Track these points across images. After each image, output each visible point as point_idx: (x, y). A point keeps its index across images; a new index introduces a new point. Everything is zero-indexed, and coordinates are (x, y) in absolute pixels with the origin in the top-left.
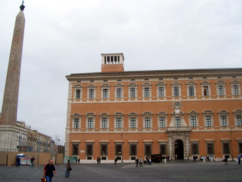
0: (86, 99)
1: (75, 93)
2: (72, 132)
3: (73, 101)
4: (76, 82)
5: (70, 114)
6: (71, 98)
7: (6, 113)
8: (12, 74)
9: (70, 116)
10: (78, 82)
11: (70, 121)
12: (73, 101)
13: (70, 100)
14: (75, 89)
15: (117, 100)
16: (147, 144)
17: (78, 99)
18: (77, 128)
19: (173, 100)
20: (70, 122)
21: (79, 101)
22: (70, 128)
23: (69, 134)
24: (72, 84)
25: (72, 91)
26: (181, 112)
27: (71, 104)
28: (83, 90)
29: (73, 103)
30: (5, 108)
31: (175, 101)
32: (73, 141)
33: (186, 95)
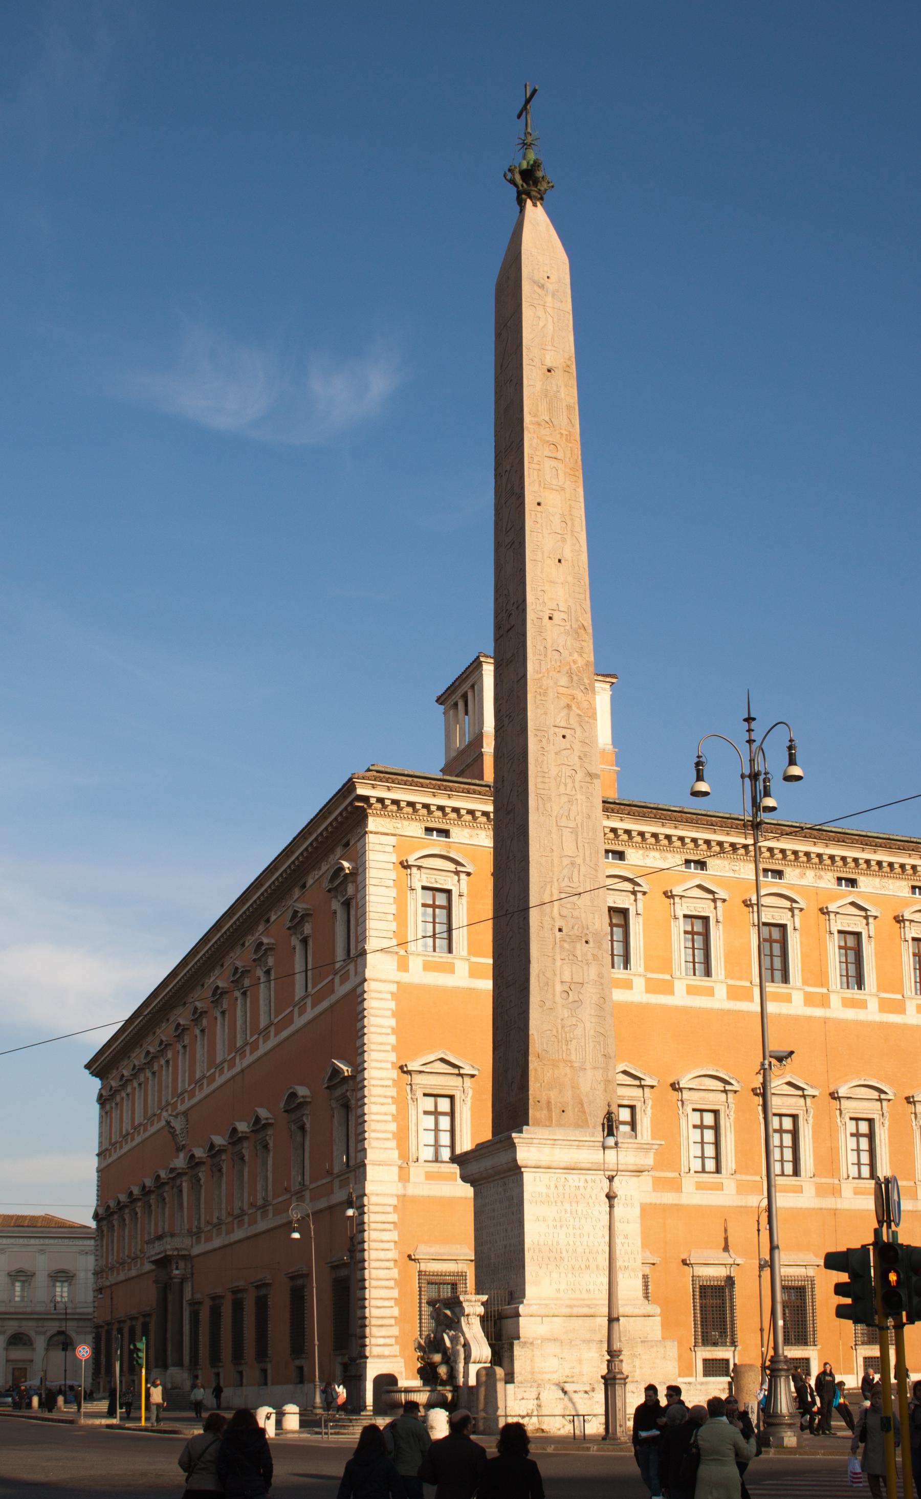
2: (412, 1190)
3: (403, 966)
4: (415, 829)
5: (393, 1057)
7: (578, 1031)
9: (395, 1074)
10: (429, 830)
11: (393, 1109)
12: (403, 966)
20: (395, 1118)
21: (450, 969)
24: (392, 840)
25: (393, 893)
29: (405, 978)
30: (559, 988)
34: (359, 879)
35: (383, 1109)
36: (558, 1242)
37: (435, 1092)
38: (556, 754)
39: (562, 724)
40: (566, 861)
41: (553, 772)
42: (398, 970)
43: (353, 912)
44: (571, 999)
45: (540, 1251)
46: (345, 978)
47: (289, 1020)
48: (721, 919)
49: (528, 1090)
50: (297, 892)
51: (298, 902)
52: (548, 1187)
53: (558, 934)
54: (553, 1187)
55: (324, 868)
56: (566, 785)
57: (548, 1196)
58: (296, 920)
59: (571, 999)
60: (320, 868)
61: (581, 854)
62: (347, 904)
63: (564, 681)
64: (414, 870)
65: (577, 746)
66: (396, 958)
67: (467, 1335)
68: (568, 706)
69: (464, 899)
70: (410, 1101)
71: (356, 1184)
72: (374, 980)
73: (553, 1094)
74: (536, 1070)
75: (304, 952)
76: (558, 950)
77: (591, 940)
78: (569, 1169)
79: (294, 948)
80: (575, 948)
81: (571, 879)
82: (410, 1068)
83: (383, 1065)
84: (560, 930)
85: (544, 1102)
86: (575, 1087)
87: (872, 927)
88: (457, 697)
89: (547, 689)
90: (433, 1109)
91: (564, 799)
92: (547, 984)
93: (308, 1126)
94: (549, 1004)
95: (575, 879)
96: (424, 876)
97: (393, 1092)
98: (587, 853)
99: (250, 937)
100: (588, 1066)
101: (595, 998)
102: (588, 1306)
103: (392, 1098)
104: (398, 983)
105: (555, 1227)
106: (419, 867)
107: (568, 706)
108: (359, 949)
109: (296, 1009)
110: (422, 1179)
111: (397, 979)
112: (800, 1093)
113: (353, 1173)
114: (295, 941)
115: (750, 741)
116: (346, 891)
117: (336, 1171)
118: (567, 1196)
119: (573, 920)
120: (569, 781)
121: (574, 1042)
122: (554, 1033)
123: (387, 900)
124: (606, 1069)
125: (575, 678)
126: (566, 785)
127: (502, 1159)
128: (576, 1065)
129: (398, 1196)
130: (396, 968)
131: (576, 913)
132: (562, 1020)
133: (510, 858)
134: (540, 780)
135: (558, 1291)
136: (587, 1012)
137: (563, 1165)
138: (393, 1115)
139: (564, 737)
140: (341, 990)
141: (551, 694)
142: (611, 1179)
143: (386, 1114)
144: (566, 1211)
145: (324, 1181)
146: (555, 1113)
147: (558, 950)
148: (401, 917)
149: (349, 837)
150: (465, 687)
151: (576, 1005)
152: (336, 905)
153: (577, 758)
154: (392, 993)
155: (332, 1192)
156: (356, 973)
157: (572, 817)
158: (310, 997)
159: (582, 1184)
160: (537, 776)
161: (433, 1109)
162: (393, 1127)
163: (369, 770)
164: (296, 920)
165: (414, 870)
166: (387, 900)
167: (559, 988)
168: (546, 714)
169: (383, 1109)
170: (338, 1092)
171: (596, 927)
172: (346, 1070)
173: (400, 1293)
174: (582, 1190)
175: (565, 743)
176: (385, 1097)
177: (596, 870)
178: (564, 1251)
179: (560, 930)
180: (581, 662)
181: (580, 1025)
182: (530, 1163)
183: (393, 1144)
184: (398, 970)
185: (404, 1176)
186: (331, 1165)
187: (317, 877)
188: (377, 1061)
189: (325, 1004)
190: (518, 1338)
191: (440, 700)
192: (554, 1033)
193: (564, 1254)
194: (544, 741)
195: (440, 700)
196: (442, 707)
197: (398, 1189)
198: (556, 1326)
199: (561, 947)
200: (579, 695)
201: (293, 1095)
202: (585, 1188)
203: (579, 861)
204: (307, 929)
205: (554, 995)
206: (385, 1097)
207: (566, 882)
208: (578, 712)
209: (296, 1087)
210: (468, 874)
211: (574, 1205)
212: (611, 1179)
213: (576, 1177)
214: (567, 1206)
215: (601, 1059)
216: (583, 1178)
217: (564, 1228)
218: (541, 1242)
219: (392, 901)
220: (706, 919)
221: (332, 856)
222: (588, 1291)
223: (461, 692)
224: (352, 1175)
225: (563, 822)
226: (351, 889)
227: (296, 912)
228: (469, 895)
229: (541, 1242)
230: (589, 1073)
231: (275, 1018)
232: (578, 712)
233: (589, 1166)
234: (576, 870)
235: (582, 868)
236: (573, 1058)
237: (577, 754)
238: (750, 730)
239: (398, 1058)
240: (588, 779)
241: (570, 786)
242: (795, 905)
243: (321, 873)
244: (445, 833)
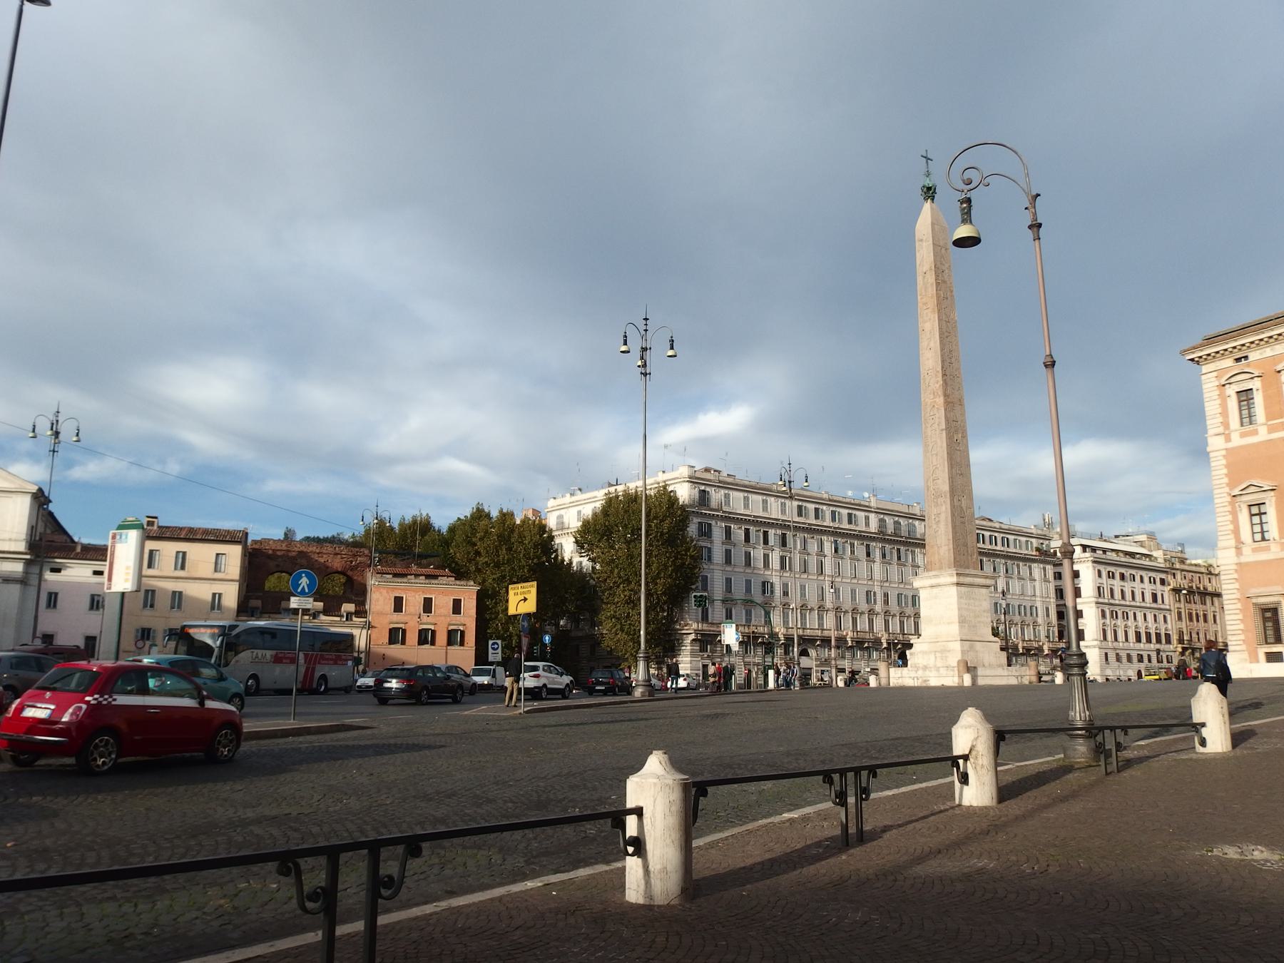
1: (1233, 403)
2: (1243, 559)
3: (1228, 439)
4: (1228, 362)
5: (1227, 489)
6: (1221, 430)
7: (940, 532)
8: (935, 412)
9: (1229, 499)
10: (1238, 360)
11: (1230, 517)
12: (1228, 439)
14: (1231, 391)
17: (1248, 428)
18: (1263, 539)
21: (1255, 433)
23: (1235, 567)
24: (1215, 374)
25: (1218, 402)
28: (1265, 388)
29: (1230, 445)
32: (1253, 591)
41: (929, 434)
72: (1213, 451)
83: (1222, 495)
86: (939, 554)
100: (943, 544)
103: (1229, 511)
104: (1226, 449)
107: (934, 406)
111: (1225, 447)
129: (1237, 564)
130: (1224, 441)
148: (1225, 413)
162: (1231, 527)
180: (938, 386)
197: (1235, 560)
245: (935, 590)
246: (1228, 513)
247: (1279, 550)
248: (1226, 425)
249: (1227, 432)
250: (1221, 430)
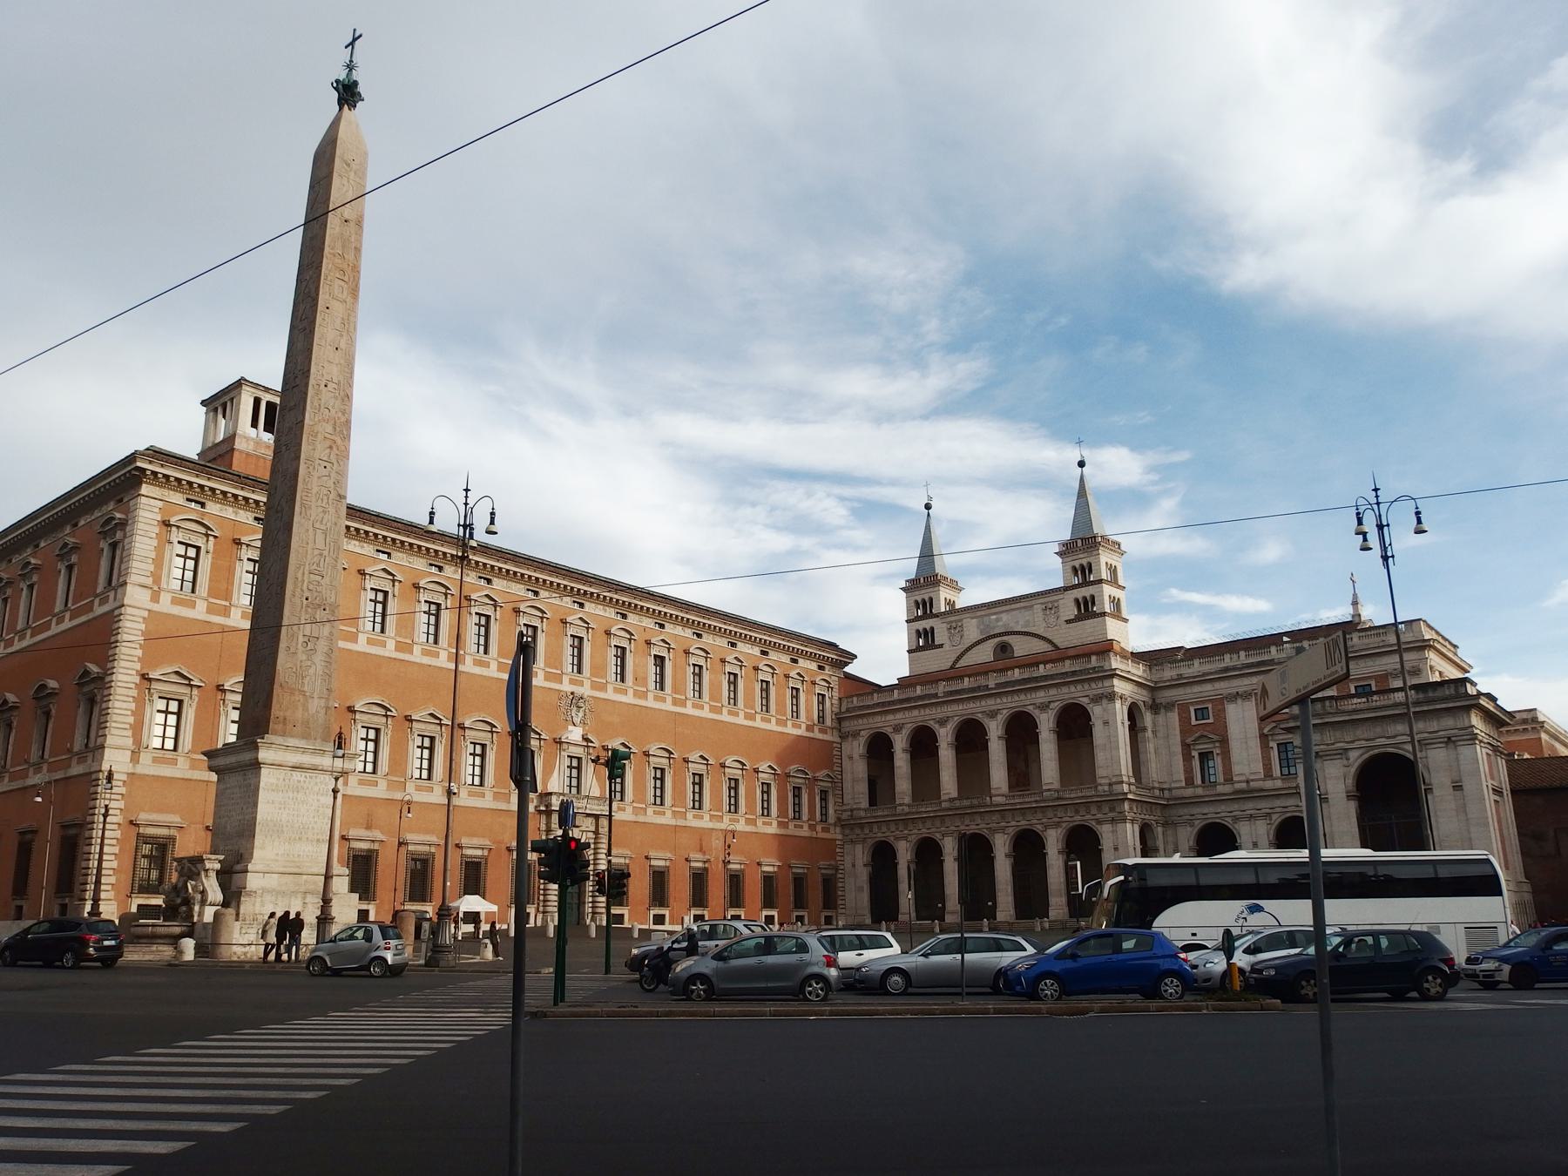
0: (224, 603)
2: (139, 770)
3: (155, 598)
4: (178, 498)
5: (138, 666)
6: (149, 581)
7: (311, 671)
9: (137, 679)
12: (155, 598)
13: (145, 590)
15: (370, 642)
16: (471, 857)
19: (566, 687)
20: (134, 713)
22: (129, 742)
24: (160, 504)
26: (586, 739)
27: (146, 614)
29: (155, 607)
30: (301, 639)
31: (572, 693)
32: (143, 817)
33: (605, 676)
34: (128, 528)
35: (125, 705)
36: (281, 820)
37: (169, 696)
38: (319, 478)
39: (324, 459)
40: (316, 552)
42: (151, 601)
43: (118, 552)
44: (309, 648)
45: (267, 825)
46: (104, 601)
47: (47, 626)
48: (396, 594)
49: (270, 709)
50: (68, 530)
51: (68, 536)
52: (278, 779)
53: (305, 602)
54: (281, 780)
55: (97, 514)
56: (322, 500)
57: (277, 785)
58: (65, 550)
59: (309, 648)
60: (92, 514)
61: (327, 548)
62: (114, 546)
63: (329, 429)
64: (174, 529)
65: (333, 475)
66: (150, 591)
67: (206, 885)
68: (331, 447)
69: (210, 556)
70: (147, 701)
71: (93, 761)
72: (130, 606)
73: (288, 714)
74: (278, 695)
75: (67, 577)
76: (303, 613)
77: (327, 609)
78: (295, 767)
79: (60, 572)
80: (316, 613)
81: (318, 565)
82: (151, 676)
83: (130, 672)
84: (307, 599)
85: (281, 719)
86: (306, 709)
87: (498, 613)
88: (217, 404)
89: (317, 433)
90: (164, 709)
91: (321, 509)
92: (293, 635)
93: (53, 711)
94: (292, 650)
95: (321, 566)
96: (180, 534)
97: (134, 693)
98: (332, 550)
99: (17, 556)
100: (315, 695)
101: (326, 649)
102: (298, 867)
103: (133, 697)
104: (149, 610)
105: (280, 809)
106: (178, 527)
107: (331, 447)
108: (121, 580)
109: (54, 620)
110: (149, 762)
111: (148, 608)
112: (438, 722)
113: (92, 753)
114: (62, 567)
115: (466, 504)
116: (115, 535)
117: (75, 749)
118: (291, 787)
119: (317, 594)
120: (325, 498)
121: (308, 678)
122: (294, 670)
123: (149, 548)
124: (327, 699)
125: (338, 429)
126: (322, 500)
127: (246, 757)
128: (307, 694)
129: (128, 774)
131: (319, 589)
132: (301, 661)
133: (276, 543)
134: (306, 494)
135: (277, 854)
136: (319, 659)
137: (290, 764)
138: (132, 711)
139: (325, 467)
140: (99, 610)
141: (320, 437)
142: (337, 779)
143: (126, 709)
144: (289, 798)
145: (64, 757)
146: (289, 726)
147: (303, 613)
148: (159, 562)
149: (122, 495)
150: (226, 398)
151: (312, 652)
152: (104, 545)
153: (332, 483)
154: (144, 618)
155: (69, 766)
156: (115, 599)
157: (324, 523)
158: (69, 612)
159: (302, 779)
160: (302, 491)
161: (164, 709)
162: (131, 720)
163: (147, 449)
164: (65, 550)
165: (174, 529)
166: (149, 548)
167: (301, 639)
168: (314, 449)
169: (125, 705)
170: (86, 689)
171: (332, 600)
172: (94, 668)
173: (120, 850)
174: (302, 783)
175: (325, 472)
176: (128, 696)
177: (336, 561)
178: (284, 825)
179: (307, 599)
181: (314, 667)
182: (267, 761)
183: (129, 733)
184: (151, 601)
185: (135, 756)
186: (72, 745)
187: (89, 520)
188: (125, 668)
189: (83, 619)
190: (245, 888)
191: (204, 403)
192: (294, 670)
193: (285, 829)
194: (311, 468)
195: (204, 403)
196: (205, 408)
197: (129, 768)
198: (272, 881)
199: (306, 612)
200: (339, 441)
201: (44, 686)
202: (305, 782)
203: (325, 553)
204: (74, 558)
205: (297, 644)
206: (128, 696)
207: (315, 567)
208: (337, 452)
209: (49, 681)
210: (215, 537)
211: (295, 793)
212: (337, 779)
213: (298, 773)
214: (291, 795)
215: (325, 691)
216: (304, 774)
217: (287, 809)
218: (269, 819)
219: (153, 548)
220: (386, 593)
221: (105, 507)
222: (299, 856)
223: (222, 401)
224: (90, 755)
225: (317, 525)
226: (119, 535)
227: (66, 545)
228: (214, 553)
229: (269, 819)
230: (316, 701)
231: (33, 623)
232: (337, 452)
233: (310, 766)
234: (322, 560)
235: (327, 558)
236: (306, 689)
237: (332, 480)
238: (466, 497)
239: (142, 668)
240: (338, 498)
241: (325, 501)
242: (448, 592)
243: (93, 518)
244: (203, 505)
245: (297, 775)
246: (131, 699)
247: (188, 768)
248: (157, 578)
249: (156, 588)
250: (149, 581)
